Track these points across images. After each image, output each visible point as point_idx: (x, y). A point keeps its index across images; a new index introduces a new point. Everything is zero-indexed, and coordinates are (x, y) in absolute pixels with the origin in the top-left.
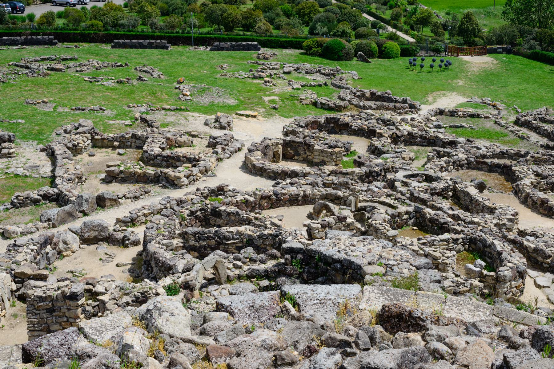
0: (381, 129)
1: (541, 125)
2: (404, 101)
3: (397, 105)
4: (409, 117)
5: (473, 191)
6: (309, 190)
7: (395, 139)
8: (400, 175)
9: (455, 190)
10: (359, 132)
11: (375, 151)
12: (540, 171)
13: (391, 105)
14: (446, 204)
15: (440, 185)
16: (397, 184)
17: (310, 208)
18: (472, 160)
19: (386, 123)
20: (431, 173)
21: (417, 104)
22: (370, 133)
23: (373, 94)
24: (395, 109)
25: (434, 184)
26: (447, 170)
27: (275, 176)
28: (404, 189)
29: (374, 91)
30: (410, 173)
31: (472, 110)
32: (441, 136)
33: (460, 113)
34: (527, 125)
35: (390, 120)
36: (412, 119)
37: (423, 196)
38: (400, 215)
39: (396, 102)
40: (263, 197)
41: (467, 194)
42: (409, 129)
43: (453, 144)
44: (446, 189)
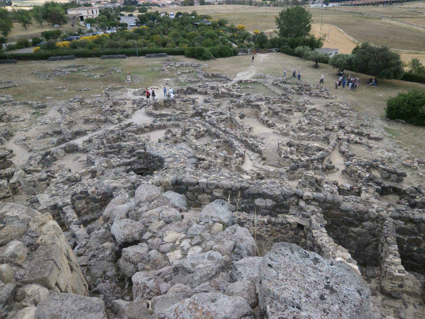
0: (210, 91)
1: (282, 85)
2: (226, 78)
3: (221, 79)
4: (225, 85)
5: (237, 118)
6: (166, 123)
7: (216, 96)
8: (209, 113)
9: (231, 118)
10: (200, 93)
11: (206, 101)
12: (271, 107)
13: (219, 79)
14: (222, 126)
15: (224, 117)
16: (206, 117)
17: (164, 131)
18: (244, 103)
19: (213, 88)
20: (223, 112)
21: (231, 79)
22: (206, 93)
23: (212, 75)
24: (220, 81)
25: (221, 116)
26: (233, 108)
27: (157, 116)
28: (207, 119)
29: (213, 73)
30: (214, 112)
31: (254, 80)
32: (235, 93)
33: (249, 81)
34: (276, 85)
35: (215, 87)
36: (227, 85)
37: (215, 122)
38: (200, 132)
39: (223, 77)
40: (146, 127)
41: (235, 120)
42: (223, 90)
43: (240, 96)
44: (226, 118)
